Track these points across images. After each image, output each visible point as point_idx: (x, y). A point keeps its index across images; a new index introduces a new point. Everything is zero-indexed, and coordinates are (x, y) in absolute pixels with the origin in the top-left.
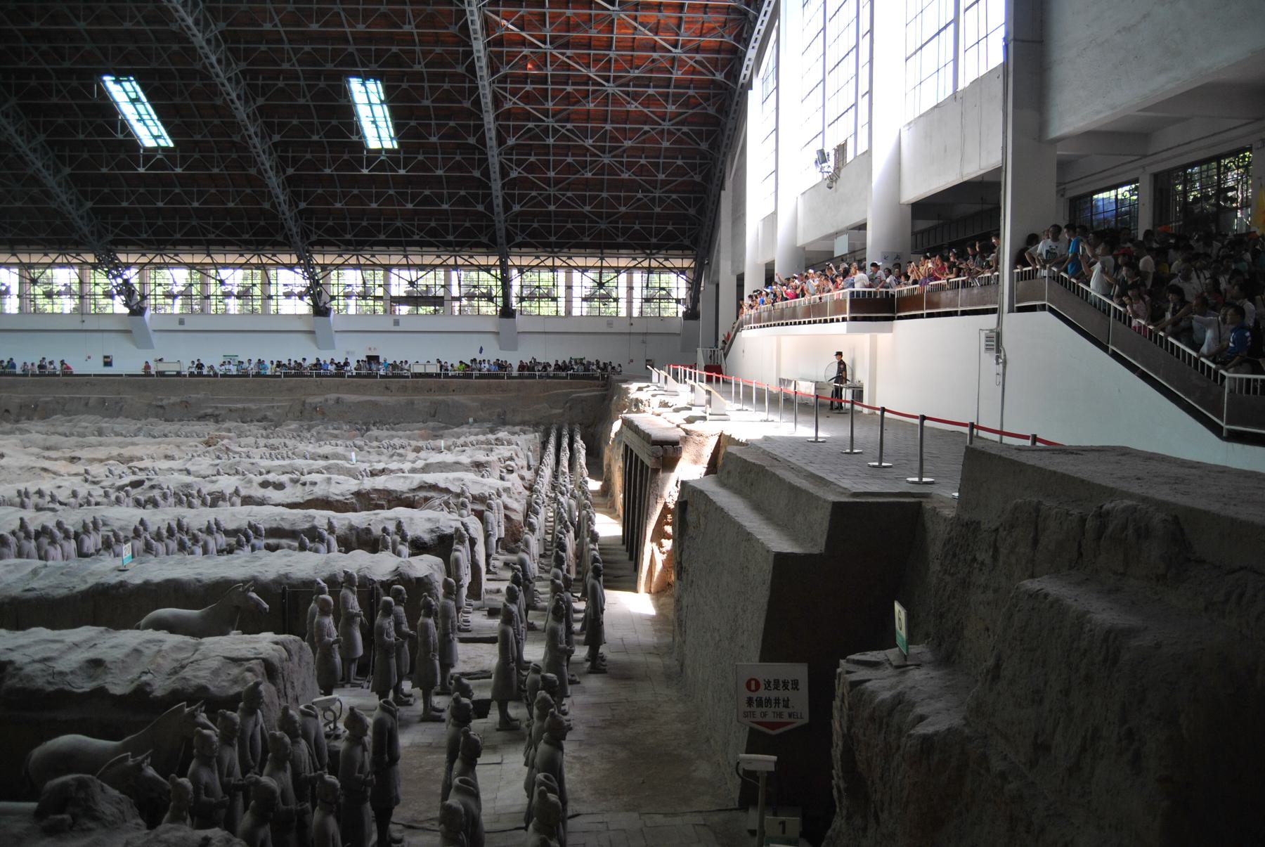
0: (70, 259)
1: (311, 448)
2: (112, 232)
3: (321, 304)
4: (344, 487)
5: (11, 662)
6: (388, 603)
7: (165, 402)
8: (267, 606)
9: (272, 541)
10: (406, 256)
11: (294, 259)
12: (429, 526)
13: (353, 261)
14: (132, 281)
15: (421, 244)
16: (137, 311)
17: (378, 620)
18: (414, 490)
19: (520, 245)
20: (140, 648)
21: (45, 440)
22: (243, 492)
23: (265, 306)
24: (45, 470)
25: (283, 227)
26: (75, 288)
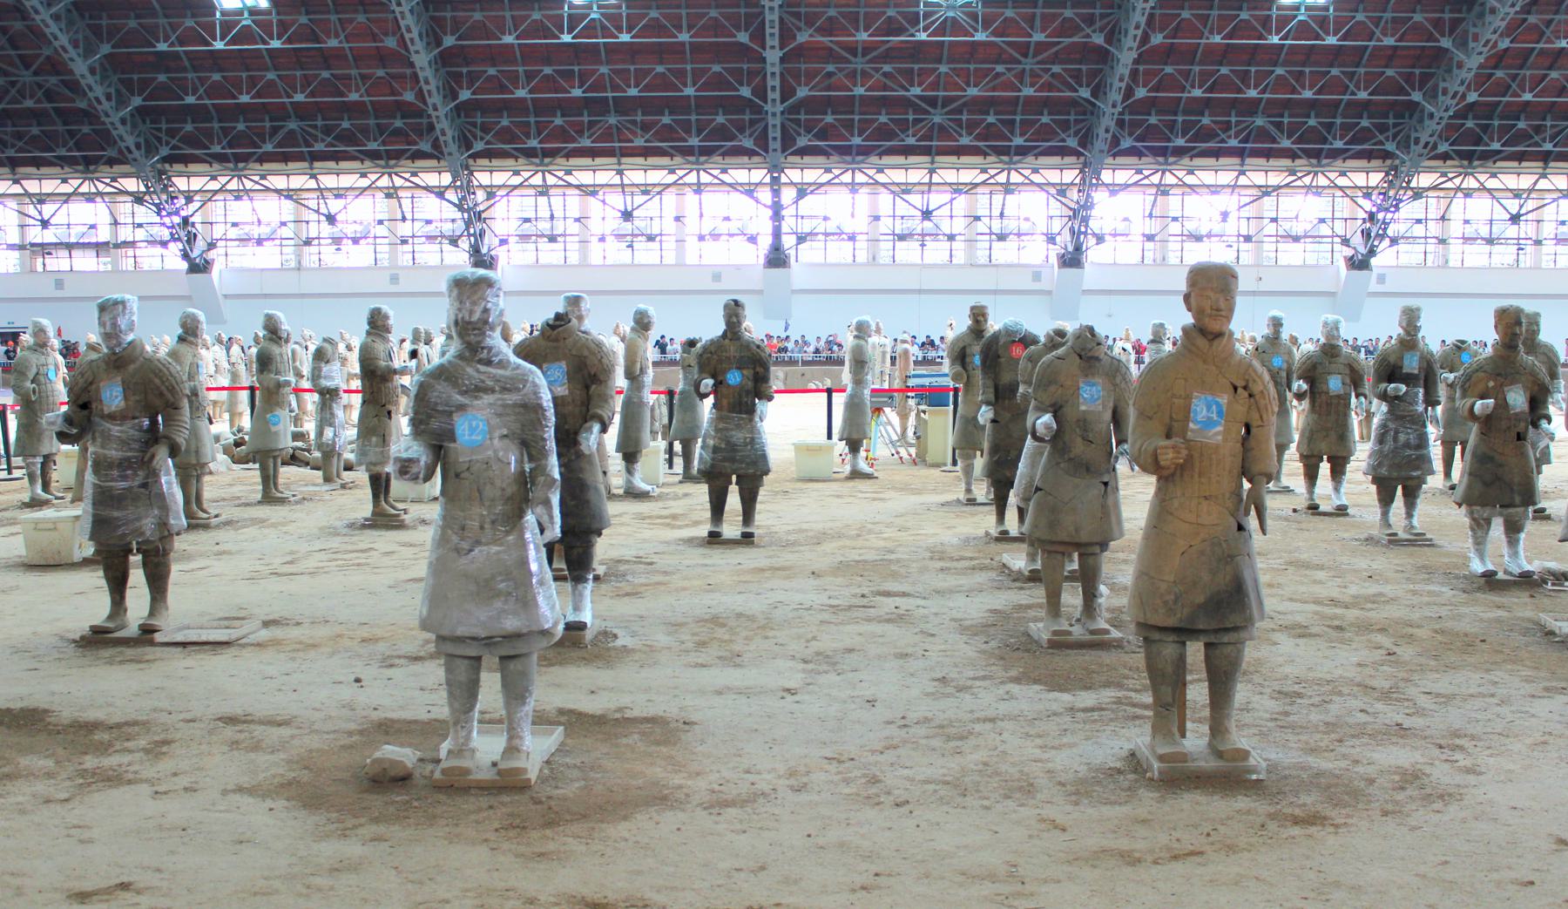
0: (101, 187)
2: (167, 143)
3: (484, 250)
10: (620, 173)
16: (199, 267)
19: (803, 152)
25: (431, 128)
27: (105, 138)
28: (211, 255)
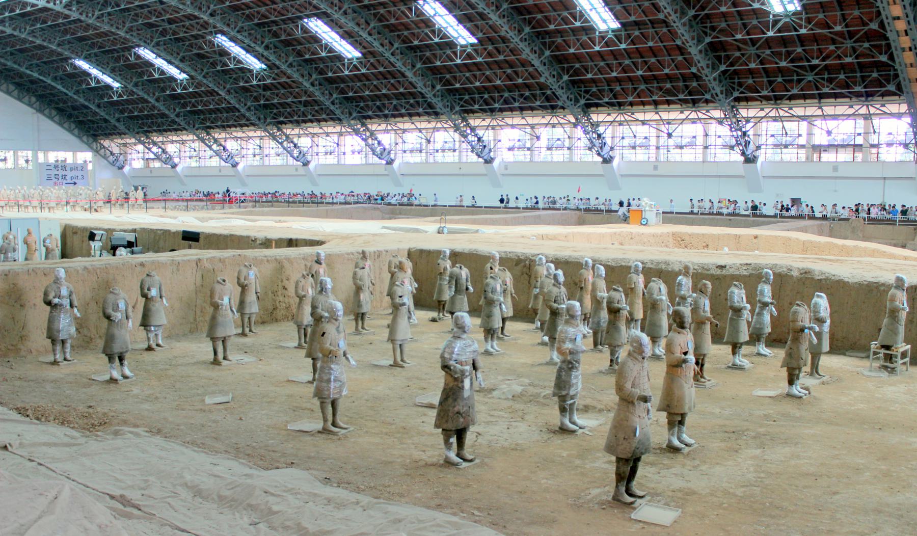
0: (700, 115)
16: (750, 160)
26: (700, 140)
27: (704, 89)
28: (757, 153)
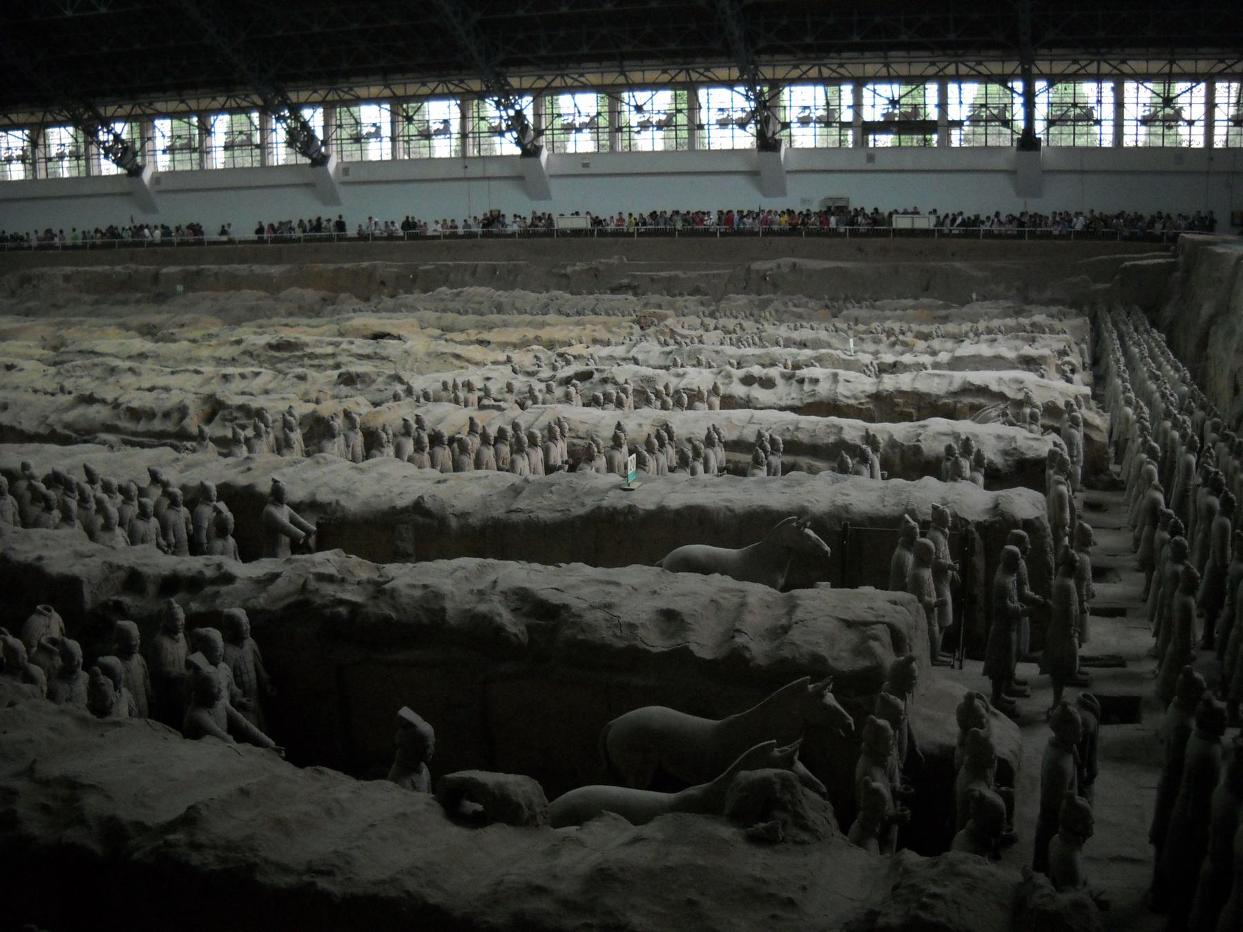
0: (452, 87)
1: (783, 331)
3: (770, 134)
4: (858, 385)
5: (565, 607)
6: (1013, 554)
7: (569, 270)
8: (827, 548)
9: (789, 459)
10: (887, 65)
11: (735, 73)
12: (1002, 445)
13: (814, 73)
14: (525, 112)
15: (908, 47)
16: (531, 152)
17: (999, 575)
18: (954, 394)
19: (1051, 45)
20: (715, 597)
21: (439, 318)
22: (722, 390)
23: (692, 138)
24: (458, 357)
26: (455, 127)
